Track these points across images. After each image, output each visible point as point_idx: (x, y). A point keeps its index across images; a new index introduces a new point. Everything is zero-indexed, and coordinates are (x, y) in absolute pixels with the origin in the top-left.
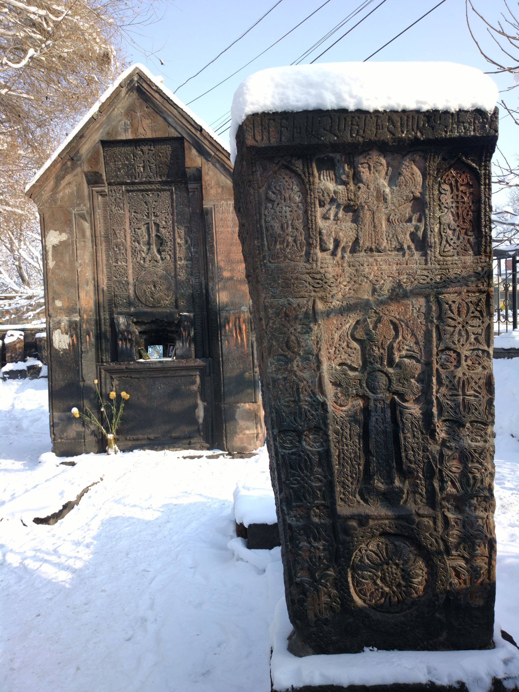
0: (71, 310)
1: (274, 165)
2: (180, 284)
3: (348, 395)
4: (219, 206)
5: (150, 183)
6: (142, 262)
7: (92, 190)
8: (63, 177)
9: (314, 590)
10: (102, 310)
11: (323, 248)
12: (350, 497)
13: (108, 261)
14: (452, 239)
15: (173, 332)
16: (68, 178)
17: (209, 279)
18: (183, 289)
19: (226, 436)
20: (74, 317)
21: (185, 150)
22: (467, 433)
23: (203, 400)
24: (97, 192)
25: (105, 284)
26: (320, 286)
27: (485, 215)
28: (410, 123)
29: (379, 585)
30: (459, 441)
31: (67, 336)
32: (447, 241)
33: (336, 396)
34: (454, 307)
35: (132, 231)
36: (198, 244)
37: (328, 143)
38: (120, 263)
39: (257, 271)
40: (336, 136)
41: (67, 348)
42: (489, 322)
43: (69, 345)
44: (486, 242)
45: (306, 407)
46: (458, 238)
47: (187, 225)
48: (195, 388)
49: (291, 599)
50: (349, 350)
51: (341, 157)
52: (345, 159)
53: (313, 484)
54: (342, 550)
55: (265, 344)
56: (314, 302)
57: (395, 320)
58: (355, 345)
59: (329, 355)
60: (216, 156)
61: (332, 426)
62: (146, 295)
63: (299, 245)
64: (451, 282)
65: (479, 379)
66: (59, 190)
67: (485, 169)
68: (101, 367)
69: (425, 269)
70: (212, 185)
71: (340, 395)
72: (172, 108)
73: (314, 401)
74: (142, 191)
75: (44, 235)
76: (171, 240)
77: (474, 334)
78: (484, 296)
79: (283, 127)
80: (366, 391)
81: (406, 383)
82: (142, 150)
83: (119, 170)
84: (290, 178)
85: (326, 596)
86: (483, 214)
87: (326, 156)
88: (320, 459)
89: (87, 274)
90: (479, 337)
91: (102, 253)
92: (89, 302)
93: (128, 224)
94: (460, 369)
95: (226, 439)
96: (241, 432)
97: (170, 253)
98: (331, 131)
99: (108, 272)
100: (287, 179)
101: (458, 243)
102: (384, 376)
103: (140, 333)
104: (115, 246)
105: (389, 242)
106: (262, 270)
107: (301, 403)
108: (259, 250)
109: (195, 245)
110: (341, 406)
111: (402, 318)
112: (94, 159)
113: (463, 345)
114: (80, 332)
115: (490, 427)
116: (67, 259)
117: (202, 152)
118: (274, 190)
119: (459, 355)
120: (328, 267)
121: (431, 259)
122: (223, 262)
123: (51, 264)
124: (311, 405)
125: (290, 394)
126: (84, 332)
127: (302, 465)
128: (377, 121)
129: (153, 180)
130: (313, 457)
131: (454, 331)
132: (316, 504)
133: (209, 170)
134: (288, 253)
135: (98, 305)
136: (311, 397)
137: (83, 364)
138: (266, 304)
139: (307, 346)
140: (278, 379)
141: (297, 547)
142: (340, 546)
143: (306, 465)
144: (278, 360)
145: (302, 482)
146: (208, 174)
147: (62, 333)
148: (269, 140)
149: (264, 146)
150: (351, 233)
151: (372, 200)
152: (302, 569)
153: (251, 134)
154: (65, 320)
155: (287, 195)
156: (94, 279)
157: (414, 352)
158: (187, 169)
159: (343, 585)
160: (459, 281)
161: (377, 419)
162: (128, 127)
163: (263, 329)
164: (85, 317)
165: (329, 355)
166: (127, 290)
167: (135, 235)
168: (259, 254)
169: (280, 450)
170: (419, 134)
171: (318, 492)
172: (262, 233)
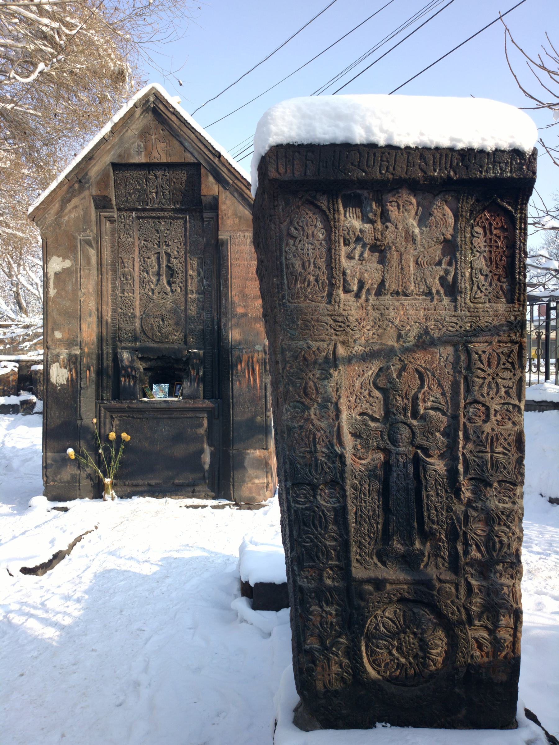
0: (71, 343)
1: (297, 200)
2: (190, 319)
3: (368, 447)
4: (236, 237)
5: (162, 210)
6: (150, 293)
7: (100, 215)
8: (70, 201)
9: (325, 659)
10: (104, 344)
11: (347, 289)
12: (367, 558)
13: (113, 291)
14: (483, 285)
15: (180, 370)
16: (75, 201)
17: (222, 315)
18: (194, 324)
19: (233, 485)
20: (74, 350)
21: (202, 176)
22: (495, 493)
23: (210, 445)
24: (105, 218)
25: (109, 315)
26: (342, 329)
27: (520, 261)
28: (443, 161)
29: (394, 655)
30: (485, 502)
31: (66, 371)
32: (478, 287)
33: (355, 447)
34: (484, 357)
35: (140, 260)
37: (356, 179)
38: (126, 294)
39: (275, 310)
40: (364, 172)
41: (66, 383)
42: (521, 375)
43: (68, 381)
44: (519, 290)
45: (323, 459)
46: (491, 285)
47: (200, 256)
48: (202, 431)
49: (299, 668)
50: (371, 399)
51: (369, 194)
52: (373, 196)
53: (328, 543)
54: (356, 616)
55: (281, 389)
56: (335, 346)
57: (421, 369)
58: (377, 393)
59: (349, 404)
60: (234, 184)
61: (350, 480)
62: (153, 329)
63: (320, 285)
64: (482, 330)
65: (509, 436)
66: (64, 213)
67: (521, 213)
68: (101, 405)
69: (454, 316)
70: (229, 215)
71: (359, 447)
72: (189, 131)
73: (332, 453)
74: (154, 218)
75: (45, 261)
77: (504, 387)
78: (517, 347)
79: (309, 160)
80: (388, 444)
81: (430, 436)
82: (155, 175)
83: (130, 195)
84: (314, 214)
85: (337, 665)
86: (517, 260)
87: (353, 193)
88: (336, 515)
89: (91, 305)
90: (510, 390)
92: (91, 335)
93: (137, 253)
94: (488, 424)
95: (234, 488)
96: (250, 481)
97: (181, 285)
98: (359, 167)
99: (113, 303)
100: (311, 215)
101: (490, 289)
102: (408, 428)
103: (145, 369)
104: (122, 276)
105: (417, 286)
106: (280, 310)
107: (318, 454)
108: (278, 288)
109: (208, 278)
110: (360, 459)
111: (428, 366)
112: (103, 182)
113: (492, 398)
114: (80, 367)
115: (519, 487)
116: (70, 288)
117: (219, 179)
118: (297, 226)
119: (488, 409)
120: (351, 310)
121: (460, 306)
122: (237, 297)
123: (52, 292)
124: (328, 457)
125: (306, 444)
126: (84, 367)
127: (317, 522)
128: (408, 158)
129: (166, 207)
130: (329, 514)
131: (483, 383)
132: (329, 564)
133: (226, 199)
134: (309, 293)
135: (101, 339)
136: (328, 449)
137: (82, 401)
138: (284, 346)
139: (326, 392)
140: (293, 428)
141: (307, 612)
142: (354, 611)
143: (320, 522)
144: (295, 407)
145: (315, 540)
146: (225, 203)
147: (61, 367)
148: (293, 173)
149: (287, 179)
150: (376, 275)
151: (400, 241)
152: (312, 635)
153: (274, 166)
154: (64, 353)
155: (310, 232)
156: (98, 310)
157: (440, 403)
158: (202, 197)
159: (356, 655)
160: (490, 330)
161: (398, 475)
162: (142, 150)
163: (280, 373)
164: (86, 351)
165: (349, 404)
166: (133, 323)
167: (144, 265)
168: (278, 292)
169: (292, 504)
170: (452, 173)
171: (332, 552)
172: (282, 271)
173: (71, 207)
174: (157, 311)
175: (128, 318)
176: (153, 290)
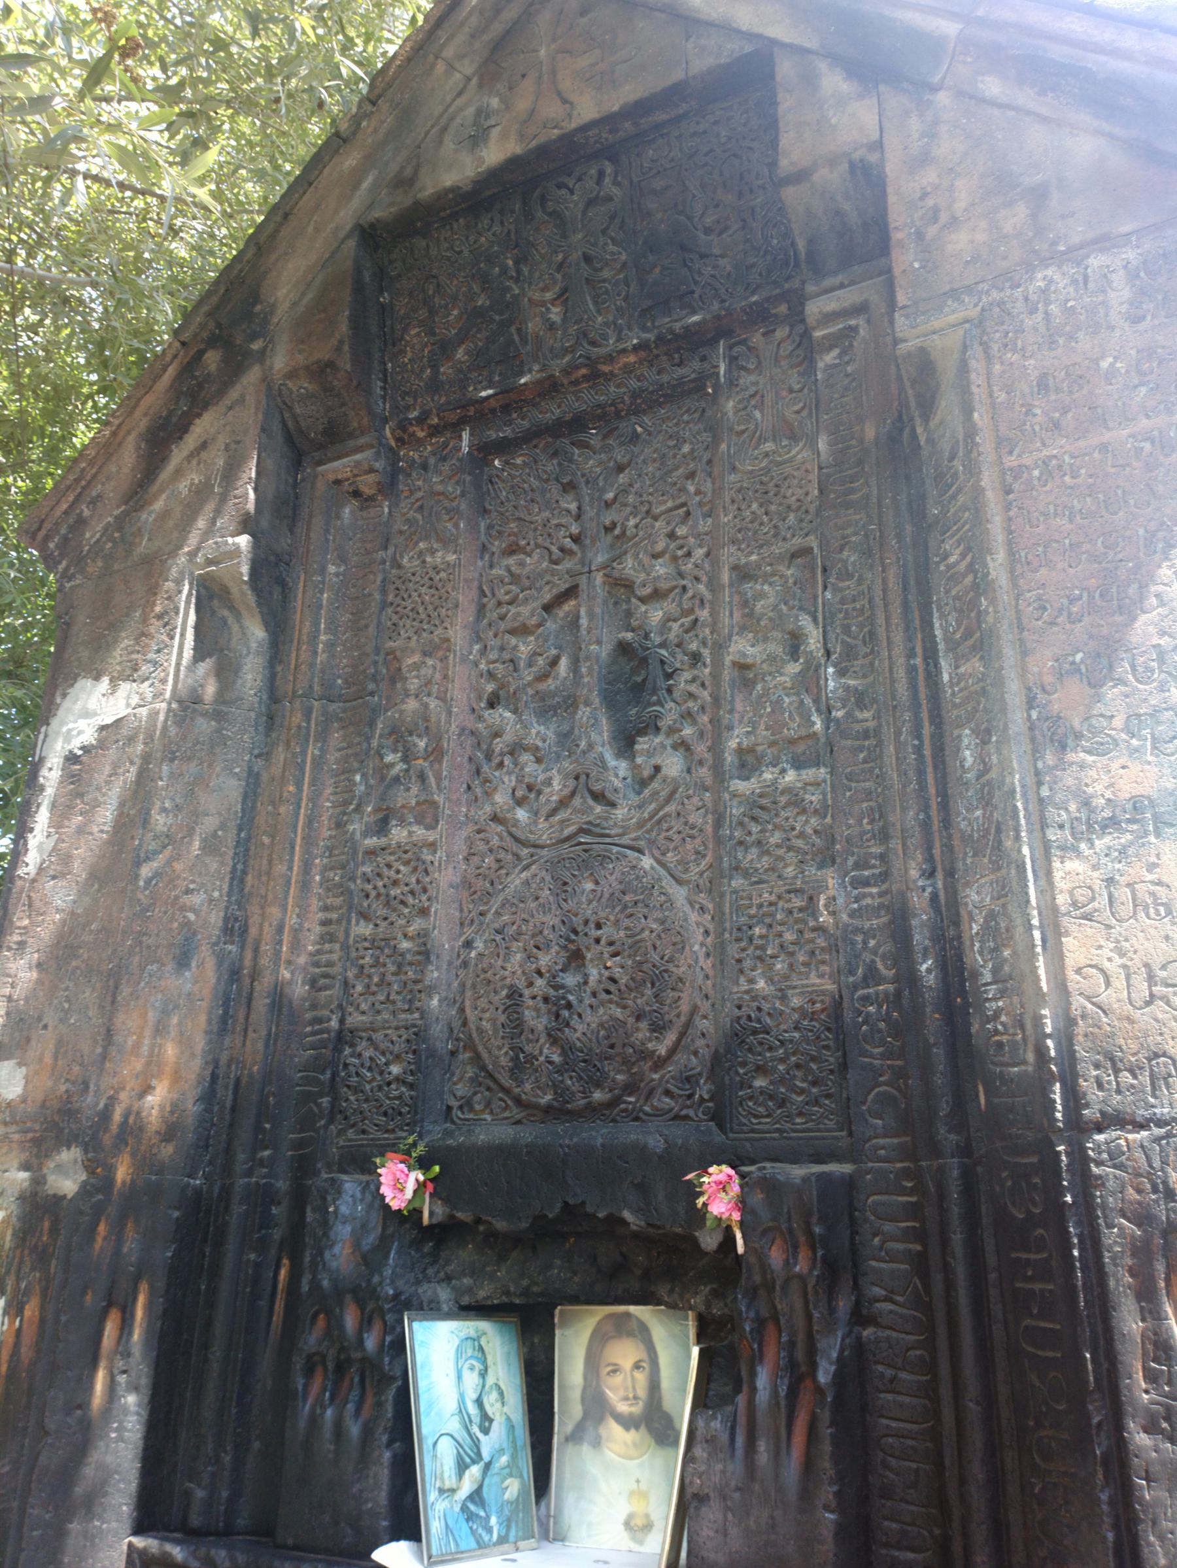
2: (742, 933)
8: (183, 429)
13: (339, 825)
16: (202, 427)
20: (59, 1168)
38: (398, 834)
47: (797, 542)
66: (154, 488)
70: (960, 206)
74: (556, 429)
76: (696, 658)
83: (445, 348)
89: (197, 899)
93: (465, 615)
109: (849, 653)
173: (185, 453)
174: (544, 908)
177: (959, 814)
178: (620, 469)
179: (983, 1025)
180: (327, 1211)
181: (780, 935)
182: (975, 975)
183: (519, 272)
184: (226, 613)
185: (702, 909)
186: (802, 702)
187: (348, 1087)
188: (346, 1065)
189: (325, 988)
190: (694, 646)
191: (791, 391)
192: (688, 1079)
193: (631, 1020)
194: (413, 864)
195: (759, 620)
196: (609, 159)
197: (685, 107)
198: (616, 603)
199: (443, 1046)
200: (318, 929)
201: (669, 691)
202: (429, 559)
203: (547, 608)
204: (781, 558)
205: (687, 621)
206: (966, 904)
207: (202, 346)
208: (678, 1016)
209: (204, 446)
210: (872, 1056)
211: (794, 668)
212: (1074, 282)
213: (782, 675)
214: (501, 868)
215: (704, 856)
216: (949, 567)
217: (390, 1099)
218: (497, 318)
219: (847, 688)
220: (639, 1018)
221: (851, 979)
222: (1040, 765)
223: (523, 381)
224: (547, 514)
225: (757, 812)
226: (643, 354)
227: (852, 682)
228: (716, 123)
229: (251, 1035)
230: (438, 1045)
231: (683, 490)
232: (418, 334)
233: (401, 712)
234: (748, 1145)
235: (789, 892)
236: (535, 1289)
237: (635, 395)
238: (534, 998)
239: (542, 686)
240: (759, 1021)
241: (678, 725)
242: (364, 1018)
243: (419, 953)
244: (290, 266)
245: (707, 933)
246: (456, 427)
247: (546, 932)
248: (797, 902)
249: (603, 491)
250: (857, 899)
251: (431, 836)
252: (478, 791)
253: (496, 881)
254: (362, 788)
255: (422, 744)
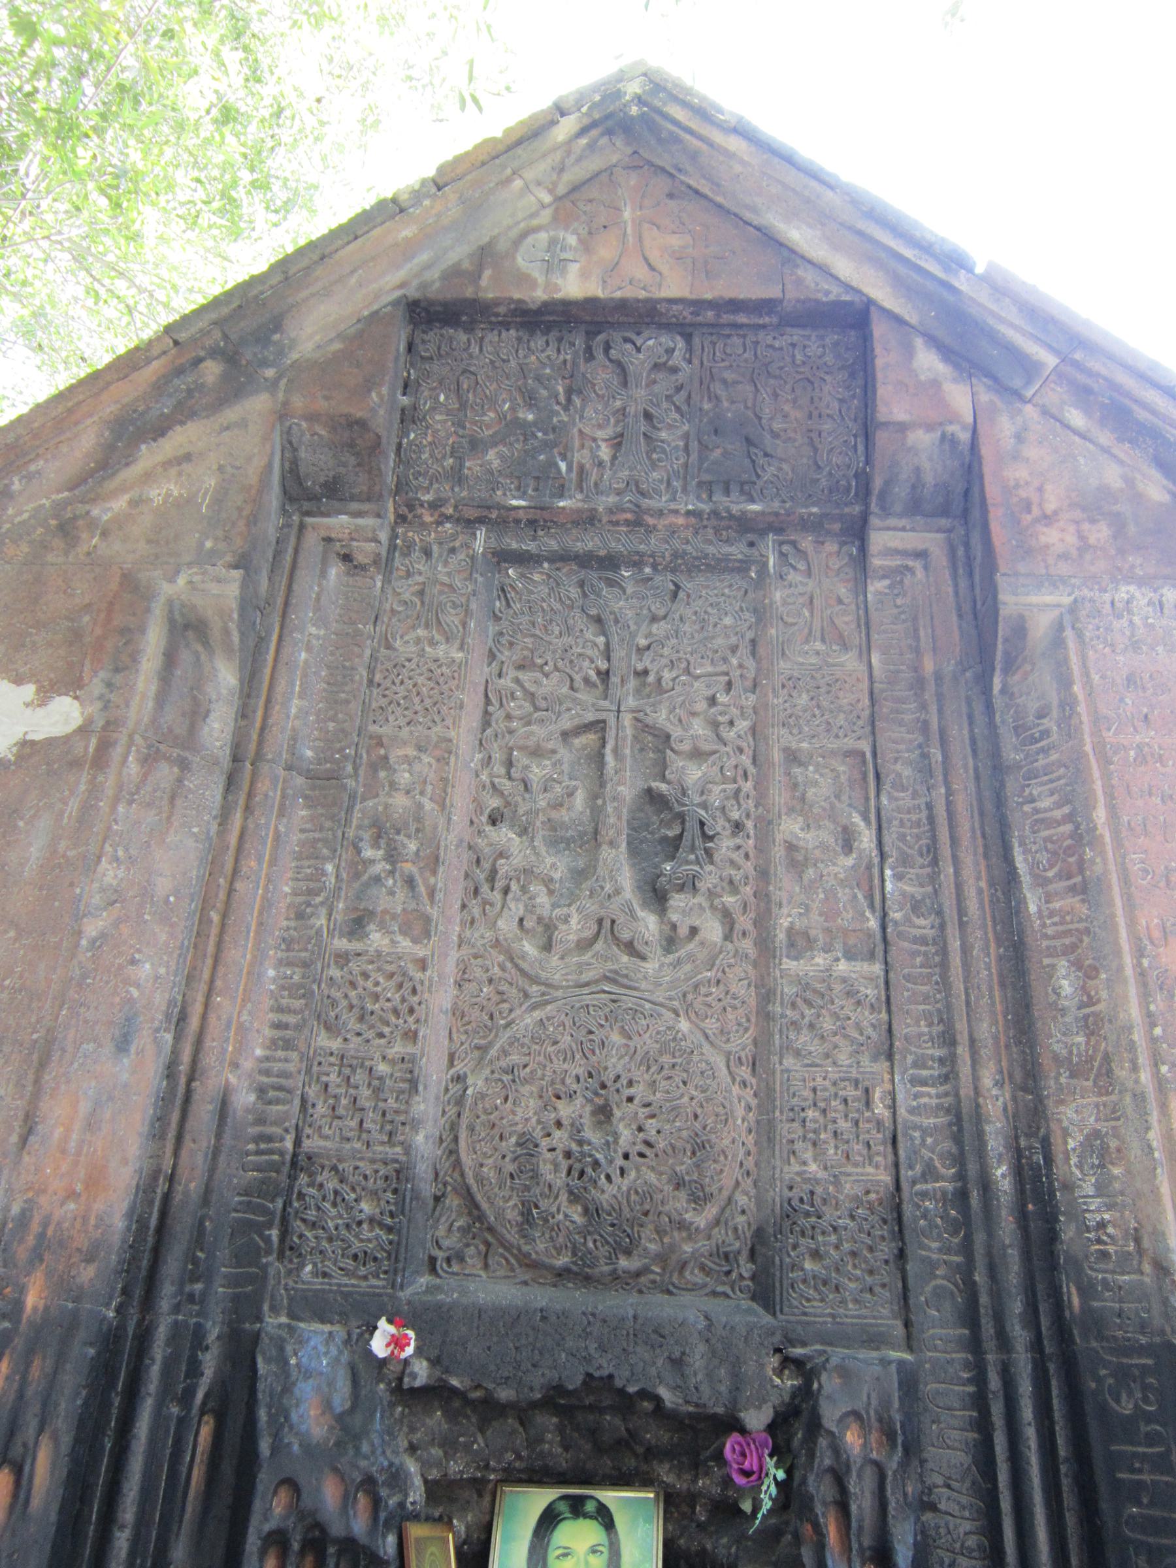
2: (796, 1114)
6: (530, 948)
8: (160, 431)
13: (300, 916)
17: (1054, 1080)
36: (932, 851)
38: (376, 939)
47: (849, 743)
62: (536, 1176)
74: (584, 560)
83: (476, 445)
91: (273, 862)
92: (95, 1180)
93: (470, 719)
97: (729, 900)
104: (366, 836)
109: (905, 860)
129: (661, 502)
146: (1016, 457)
164: (32, 1300)
167: (506, 785)
173: (159, 458)
175: (365, 1092)
176: (549, 928)
177: (1050, 1036)
178: (654, 619)
179: (1079, 1233)
180: (286, 1363)
181: (835, 1122)
182: (1068, 1187)
183: (569, 400)
184: (200, 648)
185: (744, 1084)
186: (855, 896)
187: (304, 1220)
188: (301, 1196)
189: (278, 1101)
190: (735, 815)
191: (840, 601)
192: (726, 1256)
193: (669, 1188)
194: (398, 978)
195: (811, 806)
196: (682, 334)
197: (767, 320)
198: (642, 750)
199: (428, 1189)
200: (268, 1032)
201: (709, 853)
202: (428, 649)
203: (565, 735)
204: (833, 753)
205: (731, 787)
206: (1060, 1121)
207: (202, 353)
208: (720, 1190)
209: (188, 457)
210: (929, 1249)
211: (849, 861)
212: (1150, 603)
213: (834, 864)
214: (504, 1001)
215: (746, 1030)
216: (1037, 811)
217: (362, 1241)
218: (540, 434)
219: (904, 894)
220: (678, 1186)
221: (910, 1173)
222: (1152, 1007)
223: (561, 504)
224: (570, 640)
225: (809, 995)
226: (693, 520)
227: (907, 888)
228: (793, 345)
229: (188, 1144)
230: (422, 1185)
231: (725, 660)
232: (445, 421)
233: (387, 806)
234: (799, 1328)
235: (843, 1080)
236: (517, 1464)
237: (675, 555)
238: (553, 1150)
239: (554, 815)
240: (813, 1206)
241: (718, 889)
242: (328, 1144)
243: (404, 1080)
244: (322, 308)
245: (749, 1108)
246: (470, 524)
247: (568, 1081)
248: (851, 1092)
249: (633, 636)
250: (916, 1096)
251: (420, 952)
252: (476, 911)
253: (496, 1015)
254: (333, 881)
255: (413, 846)
